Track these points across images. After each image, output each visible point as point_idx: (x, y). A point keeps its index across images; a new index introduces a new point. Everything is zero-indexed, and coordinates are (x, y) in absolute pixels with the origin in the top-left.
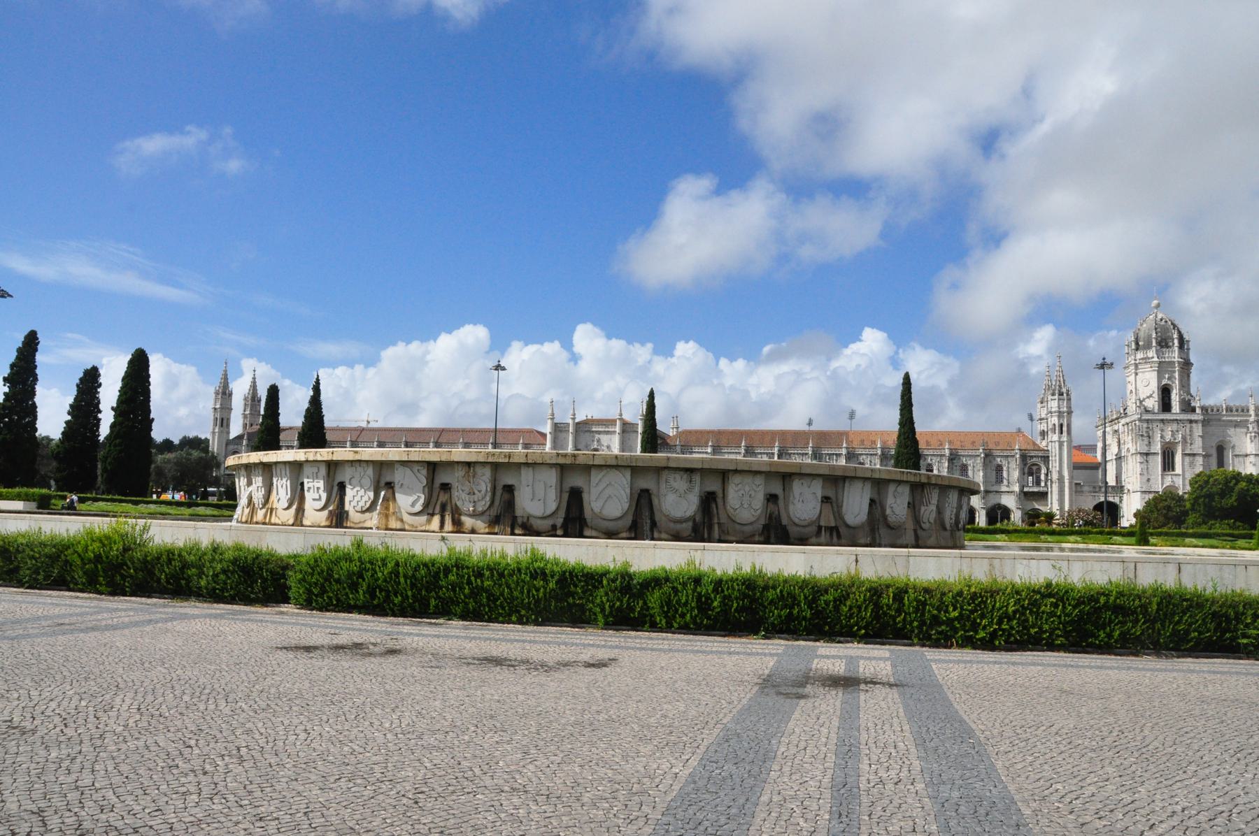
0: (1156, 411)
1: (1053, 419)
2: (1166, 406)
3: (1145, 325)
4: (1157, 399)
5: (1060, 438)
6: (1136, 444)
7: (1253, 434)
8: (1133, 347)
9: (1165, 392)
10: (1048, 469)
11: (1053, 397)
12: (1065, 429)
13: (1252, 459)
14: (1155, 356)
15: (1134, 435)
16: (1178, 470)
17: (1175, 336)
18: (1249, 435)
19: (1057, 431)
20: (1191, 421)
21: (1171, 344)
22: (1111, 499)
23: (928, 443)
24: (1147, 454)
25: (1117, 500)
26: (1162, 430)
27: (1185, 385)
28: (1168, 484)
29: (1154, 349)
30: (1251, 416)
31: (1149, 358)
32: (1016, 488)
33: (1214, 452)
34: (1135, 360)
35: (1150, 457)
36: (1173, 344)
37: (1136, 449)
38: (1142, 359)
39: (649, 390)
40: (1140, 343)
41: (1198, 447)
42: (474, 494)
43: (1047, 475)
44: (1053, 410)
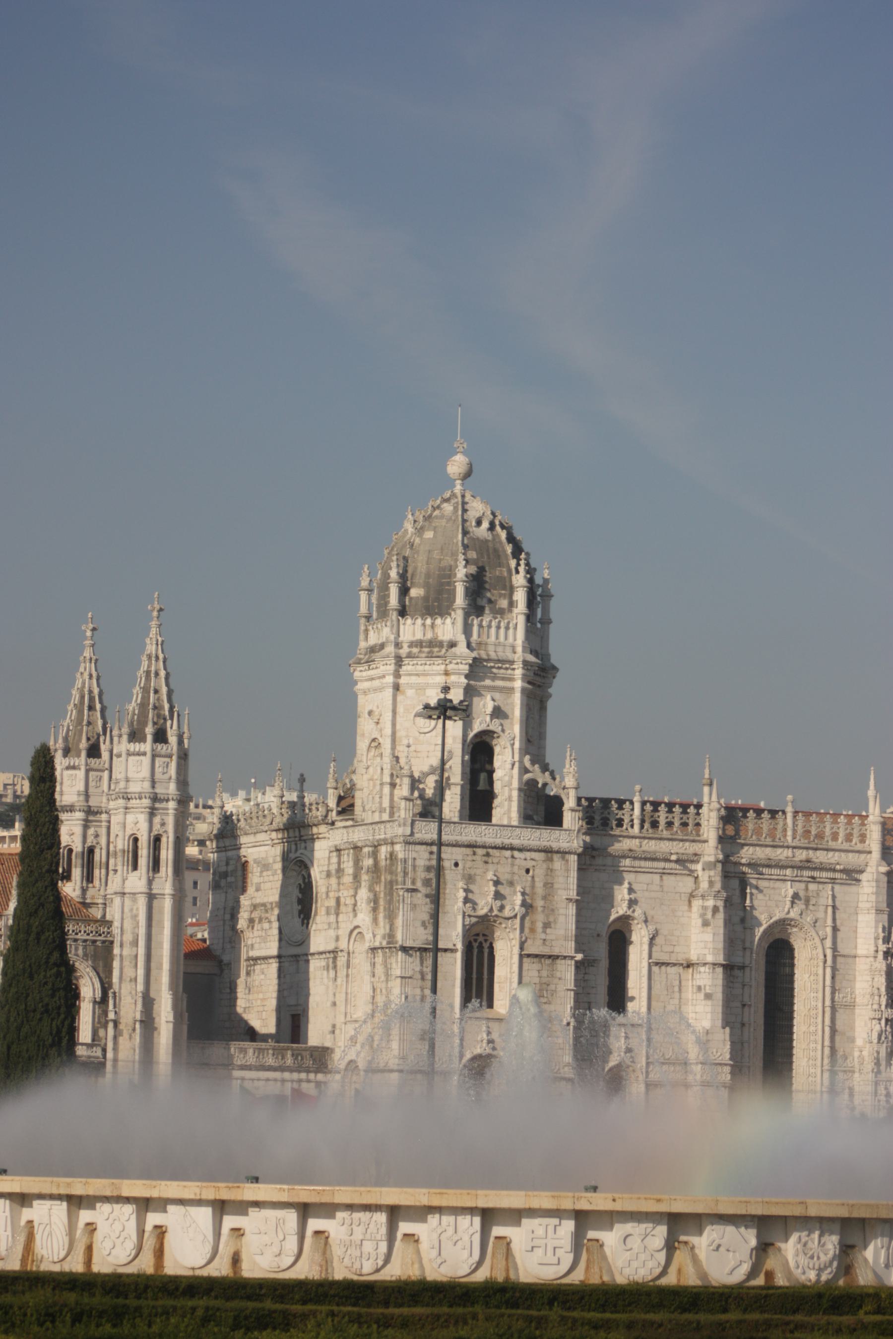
1: (130, 818)
3: (429, 535)
5: (150, 882)
6: (391, 917)
7: (710, 903)
10: (106, 987)
11: (133, 747)
12: (167, 854)
14: (461, 639)
15: (380, 888)
17: (519, 580)
18: (697, 903)
19: (143, 861)
20: (548, 851)
21: (504, 603)
26: (470, 879)
28: (478, 1051)
29: (459, 615)
31: (440, 644)
33: (602, 951)
34: (398, 645)
36: (512, 604)
37: (391, 936)
38: (419, 644)
40: (414, 592)
42: (818, 1258)
43: (102, 1002)
44: (134, 788)
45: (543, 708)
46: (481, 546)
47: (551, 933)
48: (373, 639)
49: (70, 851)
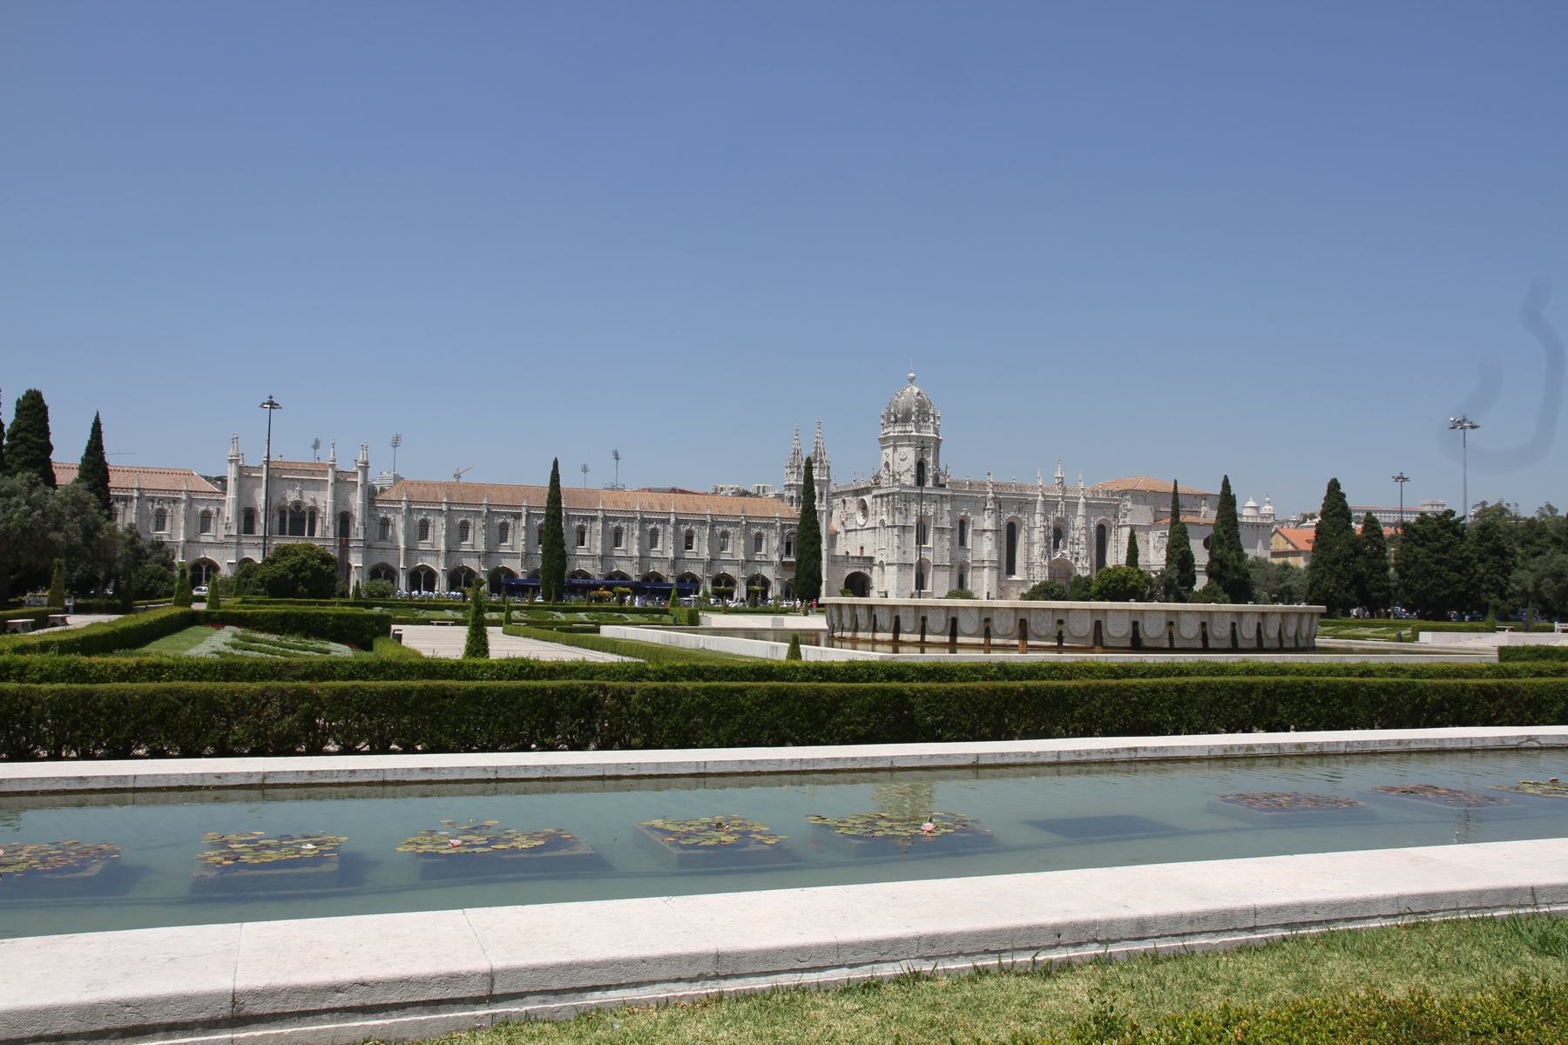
2: (920, 481)
3: (903, 398)
4: (913, 473)
6: (894, 516)
8: (893, 419)
9: (921, 466)
13: (988, 534)
14: (914, 430)
16: (930, 544)
20: (942, 496)
22: (862, 570)
24: (904, 527)
25: (867, 572)
27: (936, 461)
30: (988, 493)
31: (907, 432)
32: (776, 558)
35: (907, 529)
36: (929, 419)
37: (894, 522)
39: (554, 459)
40: (899, 416)
41: (946, 522)
45: (938, 451)
46: (918, 401)
47: (943, 520)
48: (886, 431)
49: (792, 497)
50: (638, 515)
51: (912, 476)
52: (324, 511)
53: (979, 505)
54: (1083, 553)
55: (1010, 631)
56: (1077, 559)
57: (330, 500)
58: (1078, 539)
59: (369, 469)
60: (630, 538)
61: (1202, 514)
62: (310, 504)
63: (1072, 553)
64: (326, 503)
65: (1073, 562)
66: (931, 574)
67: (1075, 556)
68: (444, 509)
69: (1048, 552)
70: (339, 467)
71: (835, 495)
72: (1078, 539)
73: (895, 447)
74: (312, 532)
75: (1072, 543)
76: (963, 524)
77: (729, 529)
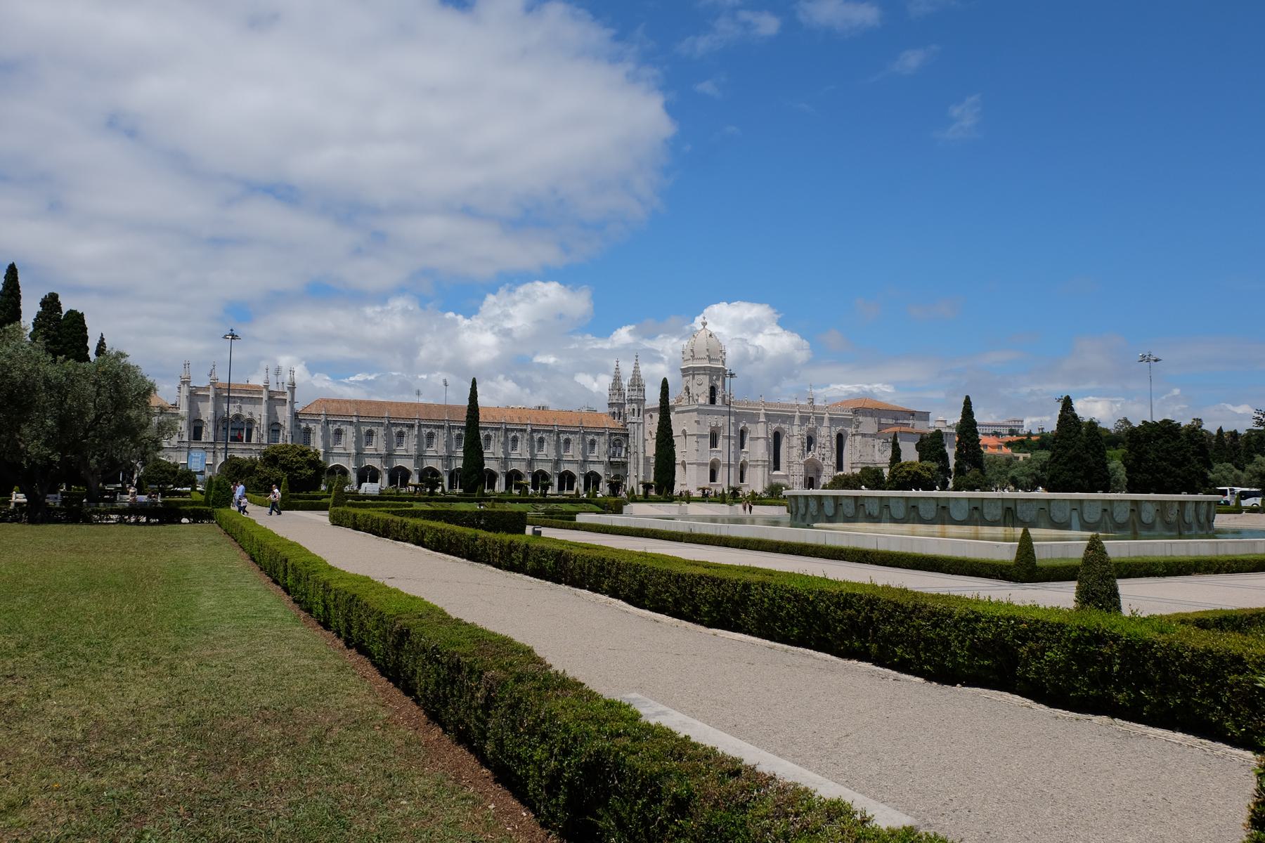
0: (707, 404)
2: (713, 401)
9: (713, 390)
23: (485, 416)
49: (614, 412)
50: (503, 426)
51: (707, 397)
52: (259, 422)
53: (753, 418)
54: (828, 455)
55: (998, 518)
56: (823, 459)
57: (264, 414)
58: (824, 444)
59: (296, 390)
60: (496, 443)
61: (911, 426)
62: (248, 416)
63: (820, 454)
64: (260, 416)
65: (821, 461)
66: (720, 469)
67: (822, 456)
68: (355, 421)
69: (804, 454)
70: (270, 389)
71: (649, 411)
72: (824, 444)
73: (694, 375)
74: (249, 439)
75: (820, 447)
76: (742, 433)
77: (570, 437)
